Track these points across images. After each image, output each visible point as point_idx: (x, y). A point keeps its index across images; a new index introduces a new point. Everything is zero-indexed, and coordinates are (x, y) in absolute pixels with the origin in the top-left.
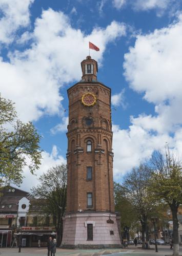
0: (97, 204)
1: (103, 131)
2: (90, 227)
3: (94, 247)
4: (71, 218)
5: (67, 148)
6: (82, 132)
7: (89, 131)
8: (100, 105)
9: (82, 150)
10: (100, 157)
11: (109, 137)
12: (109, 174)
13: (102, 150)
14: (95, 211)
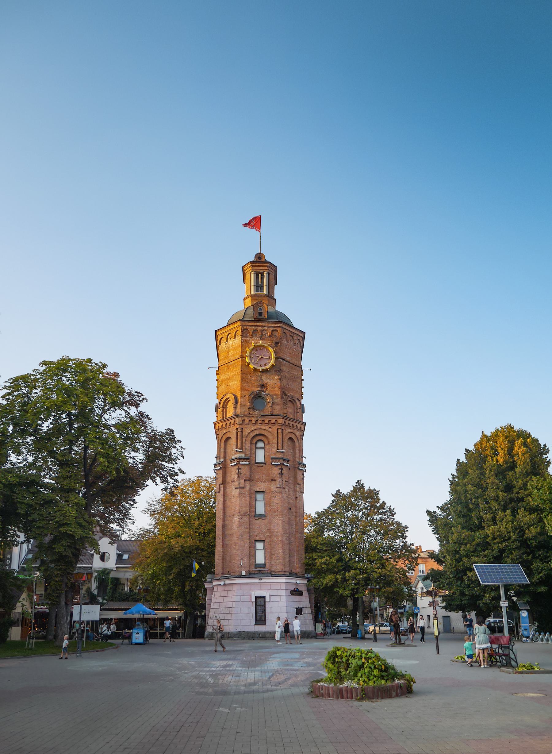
0: (273, 562)
1: (287, 422)
2: (260, 602)
3: (268, 635)
4: (225, 584)
5: (215, 453)
6: (248, 424)
7: (260, 421)
8: (284, 368)
9: (247, 459)
10: (281, 474)
11: (298, 433)
12: (296, 507)
13: (283, 459)
14: (270, 574)
